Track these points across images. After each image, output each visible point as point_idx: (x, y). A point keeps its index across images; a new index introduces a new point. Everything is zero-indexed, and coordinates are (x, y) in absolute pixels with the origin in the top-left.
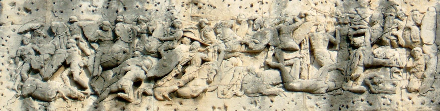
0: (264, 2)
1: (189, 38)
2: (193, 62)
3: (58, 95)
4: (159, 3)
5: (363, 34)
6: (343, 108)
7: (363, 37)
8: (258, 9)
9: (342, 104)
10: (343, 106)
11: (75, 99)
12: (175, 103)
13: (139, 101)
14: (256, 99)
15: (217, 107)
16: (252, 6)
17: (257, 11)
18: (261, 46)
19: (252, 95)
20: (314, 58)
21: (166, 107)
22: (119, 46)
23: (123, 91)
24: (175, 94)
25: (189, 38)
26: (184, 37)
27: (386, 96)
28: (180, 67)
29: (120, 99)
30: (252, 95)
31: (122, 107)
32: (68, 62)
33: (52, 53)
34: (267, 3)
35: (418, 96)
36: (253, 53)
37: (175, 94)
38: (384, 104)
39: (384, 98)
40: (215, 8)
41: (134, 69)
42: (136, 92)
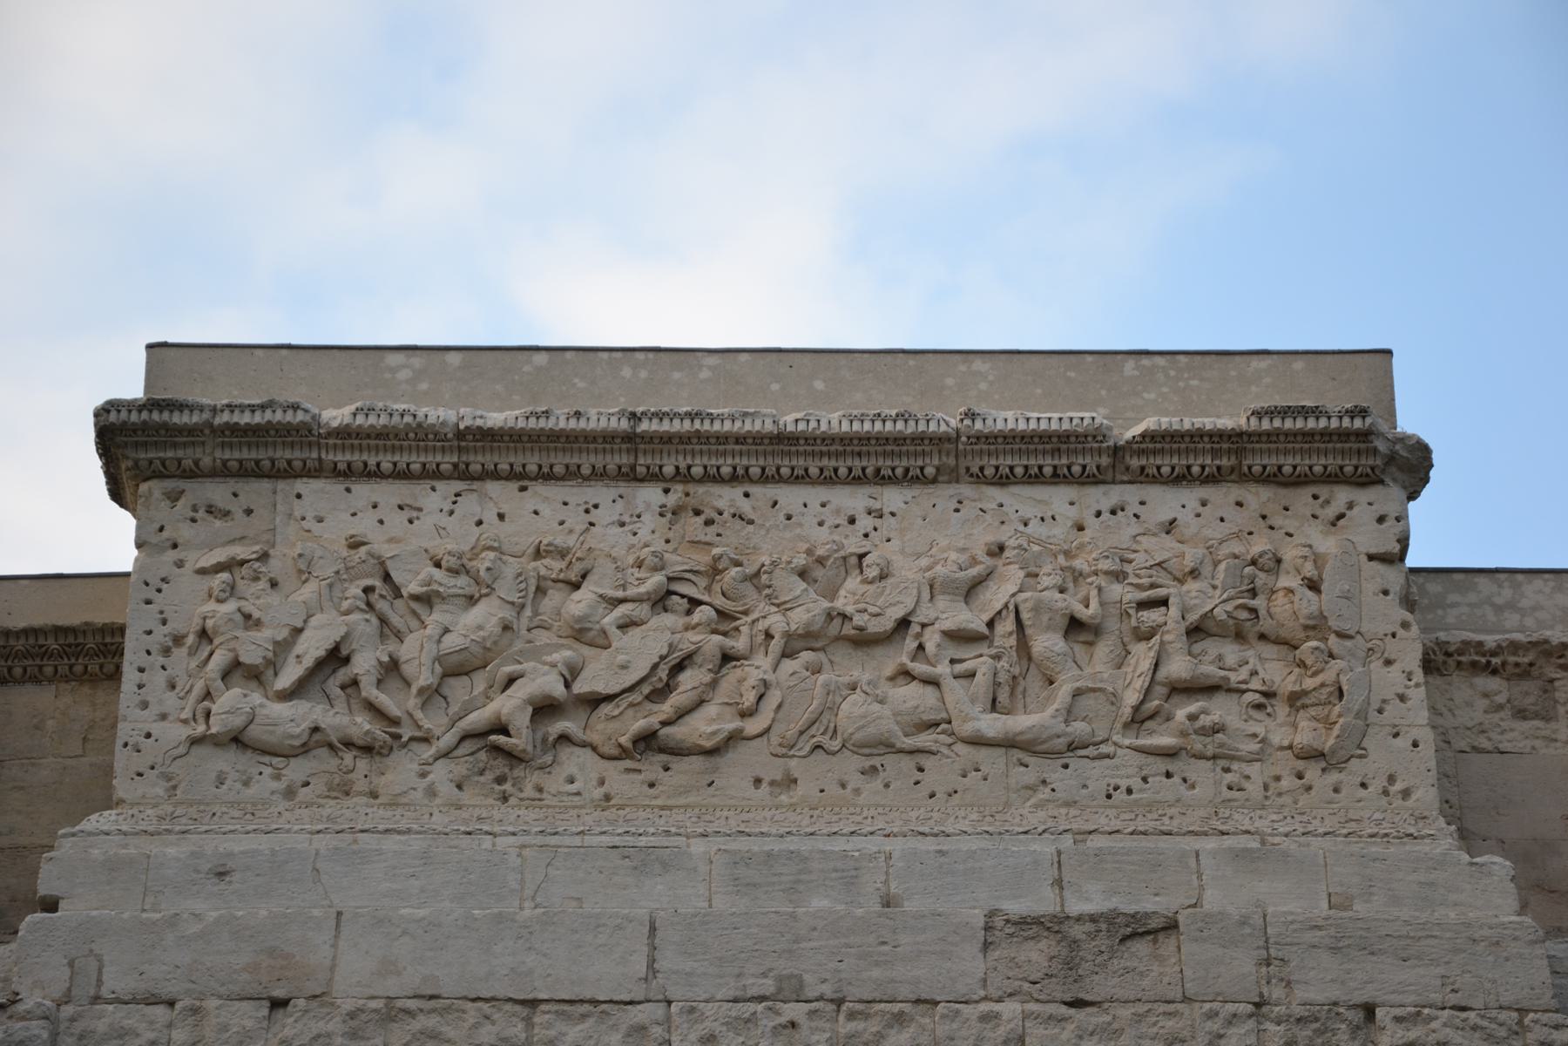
0: (886, 510)
1: (683, 596)
2: (698, 659)
3: (317, 737)
4: (596, 506)
5: (1164, 602)
6: (1116, 795)
7: (1163, 609)
8: (870, 529)
9: (1113, 782)
10: (1116, 789)
11: (367, 749)
12: (652, 766)
13: (548, 758)
14: (876, 761)
15: (767, 779)
16: (852, 521)
17: (866, 535)
18: (886, 624)
19: (867, 751)
20: (1030, 659)
21: (625, 776)
22: (483, 617)
23: (504, 730)
25: (683, 596)
26: (670, 593)
27: (1235, 766)
28: (663, 673)
29: (497, 749)
30: (867, 751)
31: (498, 773)
32: (344, 652)
33: (299, 625)
34: (893, 514)
35: (1324, 770)
37: (647, 741)
38: (1230, 788)
39: (1227, 770)
40: (751, 522)
42: (539, 735)
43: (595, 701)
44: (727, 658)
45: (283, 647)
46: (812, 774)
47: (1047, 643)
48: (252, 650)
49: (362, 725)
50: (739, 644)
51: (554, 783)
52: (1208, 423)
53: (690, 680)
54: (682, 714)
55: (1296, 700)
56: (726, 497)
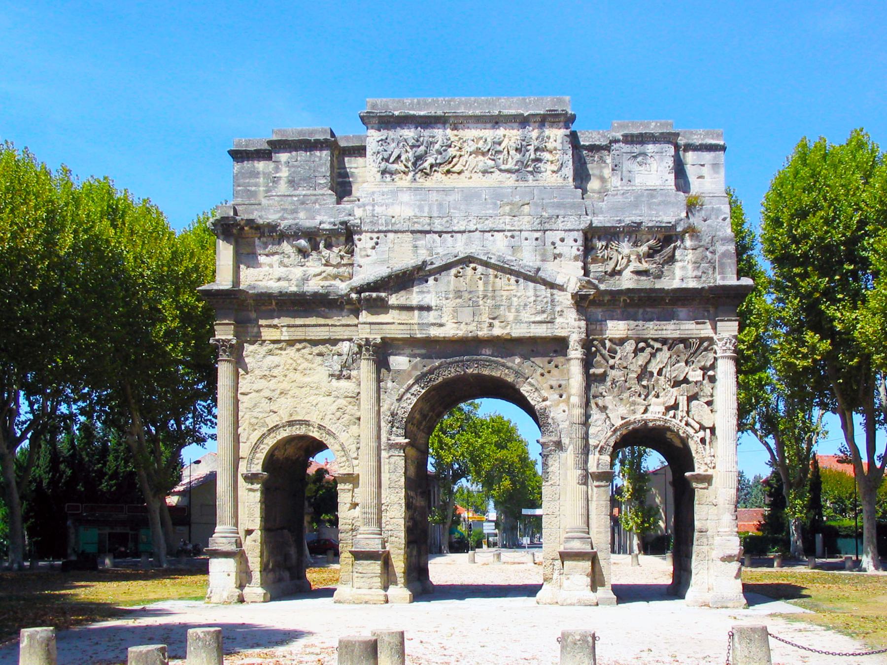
12: (449, 176)
24: (448, 172)
36: (483, 154)
37: (448, 172)
41: (430, 160)
43: (440, 164)
44: (461, 156)
45: (390, 155)
46: (474, 176)
47: (513, 152)
48: (386, 155)
49: (403, 168)
50: (462, 153)
51: (434, 178)
52: (538, 112)
53: (455, 160)
54: (454, 166)
55: (552, 162)
56: (460, 126)
